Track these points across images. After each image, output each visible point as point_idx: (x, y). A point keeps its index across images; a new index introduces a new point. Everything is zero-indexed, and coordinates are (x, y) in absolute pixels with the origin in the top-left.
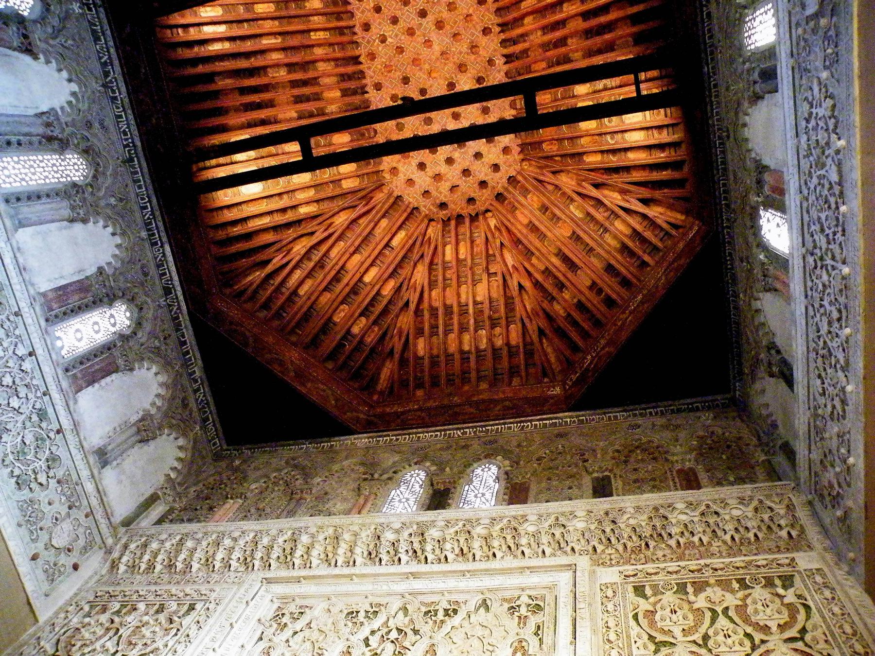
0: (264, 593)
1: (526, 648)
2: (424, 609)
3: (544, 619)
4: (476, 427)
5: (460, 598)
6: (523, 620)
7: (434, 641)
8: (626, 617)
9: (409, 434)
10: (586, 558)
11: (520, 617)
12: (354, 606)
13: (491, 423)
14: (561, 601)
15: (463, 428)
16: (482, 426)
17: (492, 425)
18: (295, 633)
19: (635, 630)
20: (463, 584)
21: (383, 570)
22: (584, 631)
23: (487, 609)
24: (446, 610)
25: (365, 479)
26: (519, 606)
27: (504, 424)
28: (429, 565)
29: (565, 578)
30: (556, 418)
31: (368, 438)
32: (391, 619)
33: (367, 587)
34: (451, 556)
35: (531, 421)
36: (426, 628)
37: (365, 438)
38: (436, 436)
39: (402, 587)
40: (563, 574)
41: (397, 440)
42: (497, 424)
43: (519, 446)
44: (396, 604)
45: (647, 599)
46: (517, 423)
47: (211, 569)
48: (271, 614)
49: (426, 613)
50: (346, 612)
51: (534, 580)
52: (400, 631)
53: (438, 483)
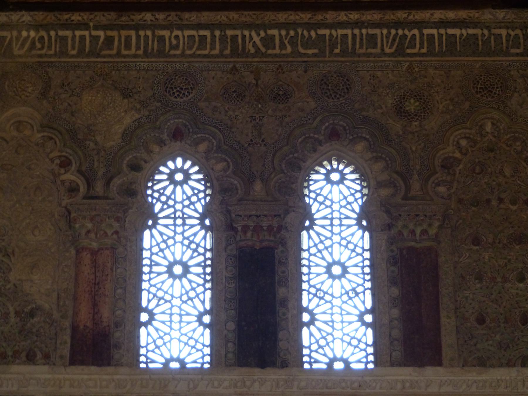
4: (295, 25)
9: (137, 28)
13: (330, 16)
15: (265, 27)
16: (309, 26)
17: (330, 26)
25: (73, 190)
27: (358, 24)
30: (476, 25)
31: (37, 27)
35: (420, 25)
37: (29, 27)
38: (203, 38)
41: (109, 41)
42: (342, 25)
43: (400, 111)
46: (389, 25)
53: (245, 229)
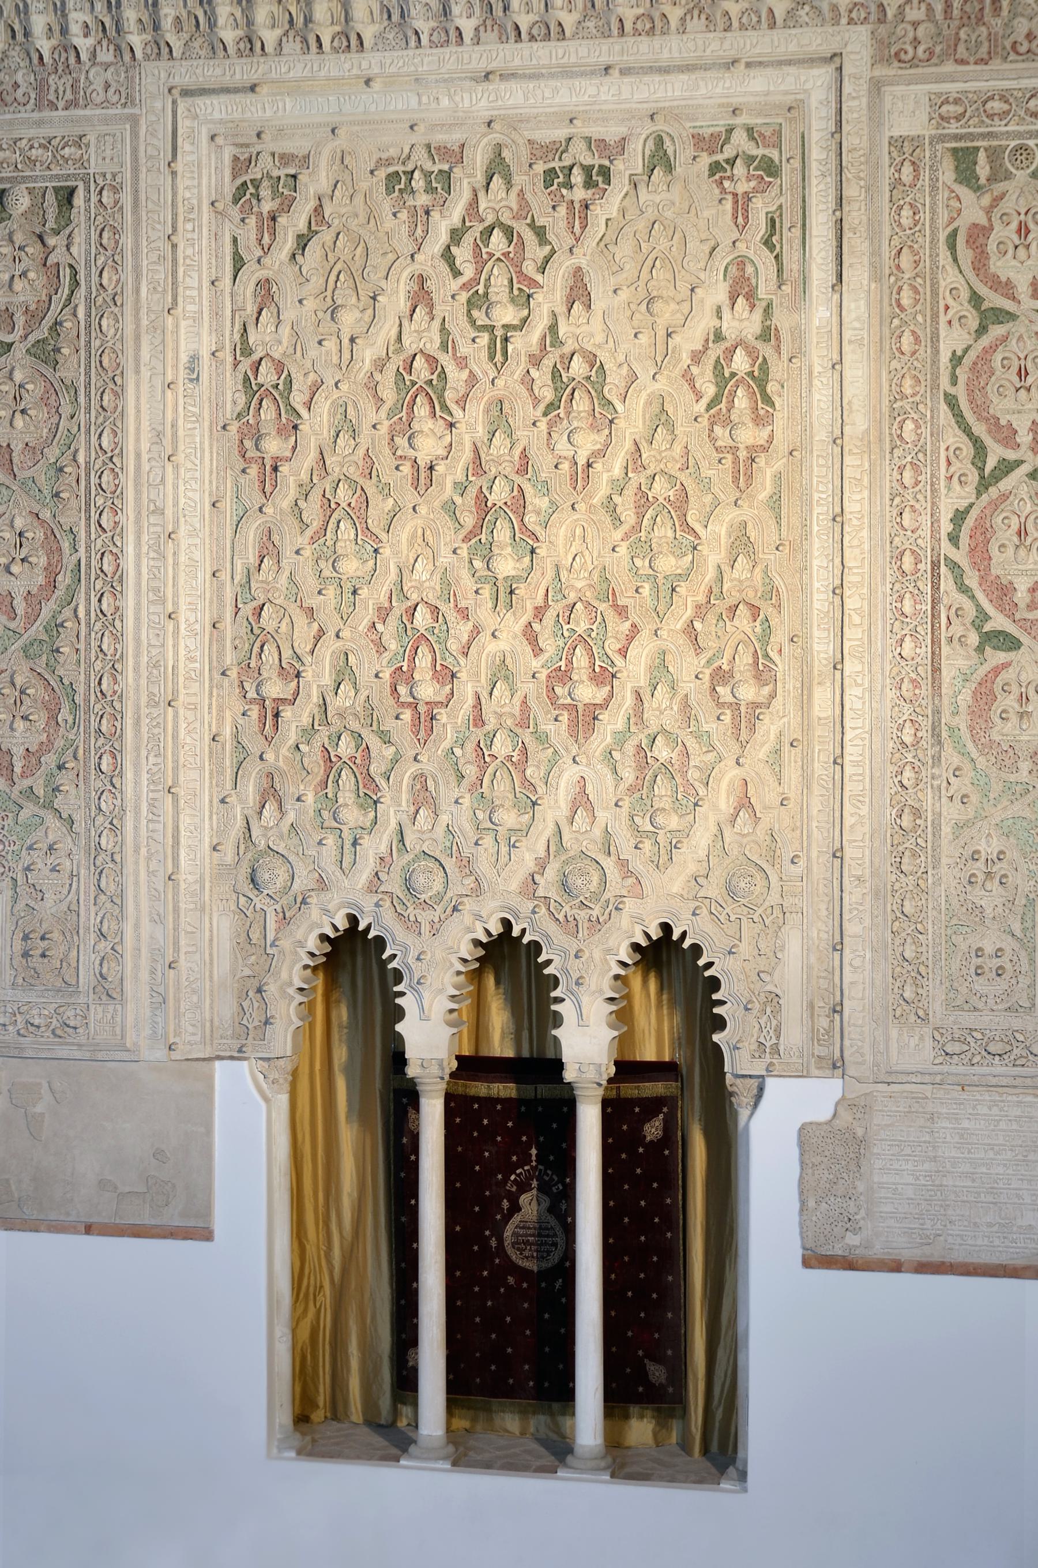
0: (188, 123)
1: (753, 281)
2: (540, 168)
3: (782, 200)
5: (611, 132)
6: (742, 205)
7: (583, 262)
8: (934, 241)
10: (863, 31)
11: (735, 195)
12: (393, 152)
14: (815, 153)
18: (303, 242)
19: (949, 278)
20: (609, 93)
21: (427, 60)
22: (857, 274)
23: (669, 168)
24: (588, 170)
26: (732, 162)
28: (525, 47)
29: (820, 77)
32: (481, 194)
33: (404, 103)
34: (569, 21)
36: (556, 222)
39: (480, 102)
40: (815, 72)
44: (479, 158)
45: (977, 189)
47: (35, 58)
48: (229, 189)
49: (550, 175)
50: (382, 174)
51: (755, 87)
52: (509, 233)
